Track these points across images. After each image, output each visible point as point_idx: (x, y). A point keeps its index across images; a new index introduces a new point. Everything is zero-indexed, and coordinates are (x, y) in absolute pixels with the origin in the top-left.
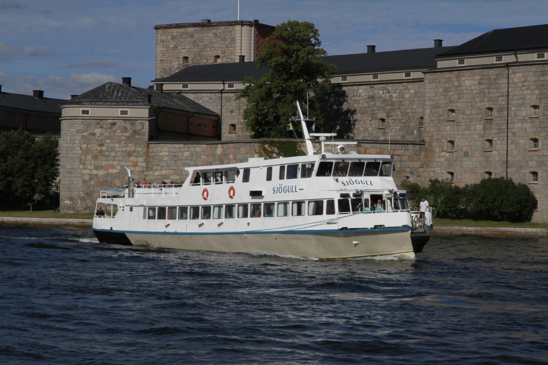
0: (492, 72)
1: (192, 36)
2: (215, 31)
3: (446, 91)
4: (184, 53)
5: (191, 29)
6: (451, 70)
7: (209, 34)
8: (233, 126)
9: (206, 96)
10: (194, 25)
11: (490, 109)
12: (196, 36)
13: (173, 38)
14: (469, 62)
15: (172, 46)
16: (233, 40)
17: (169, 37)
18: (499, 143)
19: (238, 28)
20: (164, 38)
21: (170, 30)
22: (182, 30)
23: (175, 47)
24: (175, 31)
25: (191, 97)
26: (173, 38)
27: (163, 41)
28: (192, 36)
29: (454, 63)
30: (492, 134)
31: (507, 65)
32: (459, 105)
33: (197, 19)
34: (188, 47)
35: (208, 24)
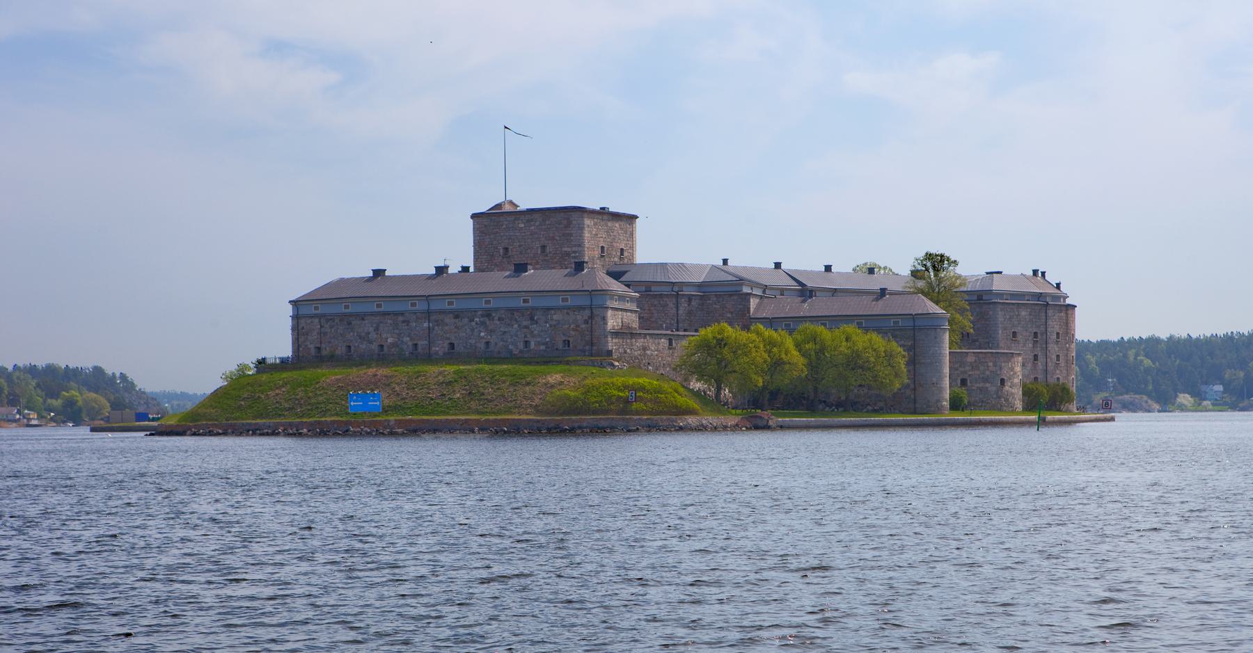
3: (1011, 318)
11: (1036, 334)
18: (1041, 358)
30: (1038, 351)
32: (1018, 329)
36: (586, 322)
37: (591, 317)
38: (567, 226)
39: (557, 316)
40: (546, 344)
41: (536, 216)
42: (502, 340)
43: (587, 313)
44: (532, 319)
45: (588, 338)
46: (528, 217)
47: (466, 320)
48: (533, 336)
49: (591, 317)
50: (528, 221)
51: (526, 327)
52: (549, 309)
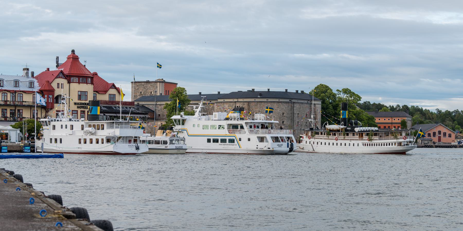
0: (232, 104)
4: (141, 91)
5: (143, 83)
6: (221, 102)
7: (149, 85)
8: (159, 115)
9: (151, 106)
10: (144, 82)
14: (226, 100)
16: (157, 87)
19: (158, 83)
23: (138, 89)
24: (138, 84)
25: (147, 106)
29: (222, 100)
31: (235, 102)
33: (145, 81)
35: (148, 82)
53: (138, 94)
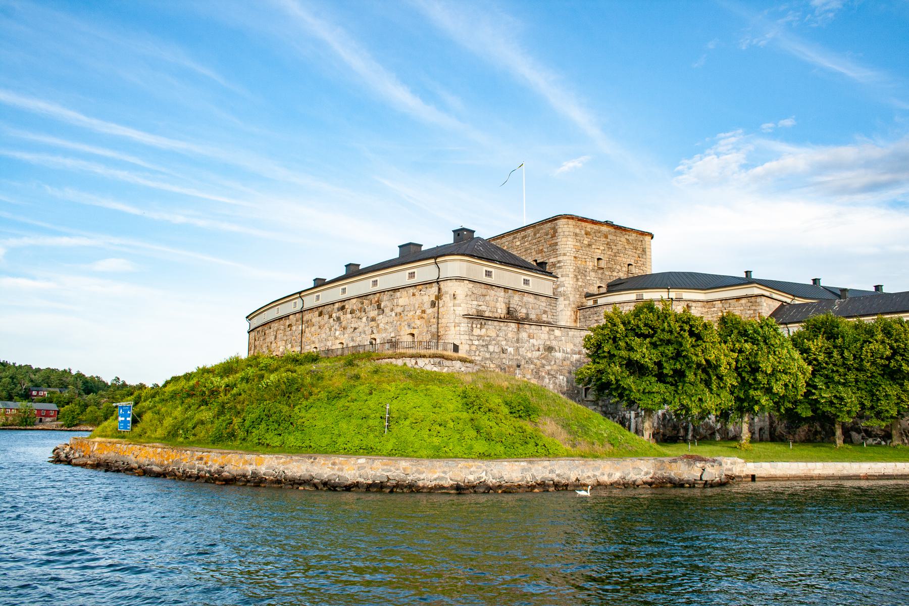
1: (606, 237)
2: (627, 237)
5: (604, 229)
7: (622, 239)
12: (610, 237)
13: (587, 234)
15: (586, 242)
17: (583, 232)
20: (578, 231)
21: (584, 224)
22: (596, 227)
23: (589, 245)
24: (589, 226)
26: (587, 234)
27: (576, 235)
28: (606, 237)
34: (602, 248)
36: (433, 304)
37: (438, 297)
38: (553, 236)
39: (403, 299)
40: (390, 342)
41: (529, 231)
42: (353, 340)
43: (434, 290)
44: (379, 307)
45: (434, 330)
46: (523, 233)
47: (327, 316)
48: (378, 332)
49: (438, 297)
50: (523, 238)
51: (373, 320)
52: (395, 290)
53: (590, 265)
